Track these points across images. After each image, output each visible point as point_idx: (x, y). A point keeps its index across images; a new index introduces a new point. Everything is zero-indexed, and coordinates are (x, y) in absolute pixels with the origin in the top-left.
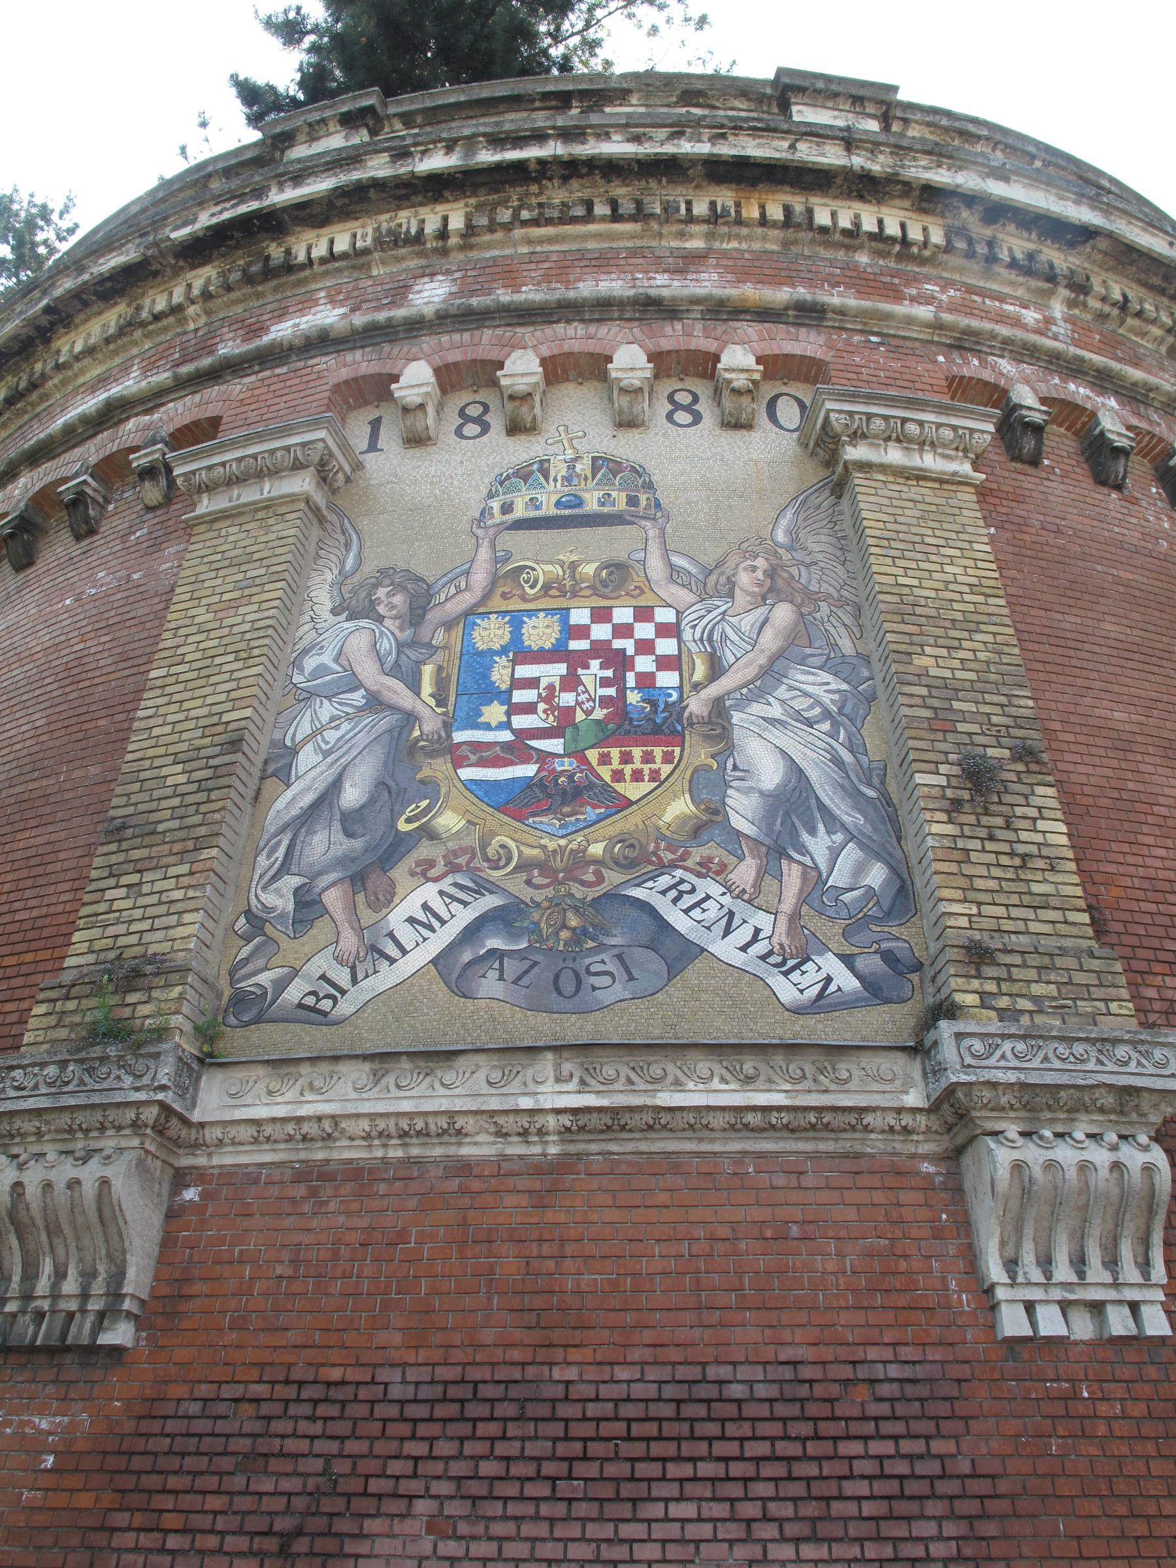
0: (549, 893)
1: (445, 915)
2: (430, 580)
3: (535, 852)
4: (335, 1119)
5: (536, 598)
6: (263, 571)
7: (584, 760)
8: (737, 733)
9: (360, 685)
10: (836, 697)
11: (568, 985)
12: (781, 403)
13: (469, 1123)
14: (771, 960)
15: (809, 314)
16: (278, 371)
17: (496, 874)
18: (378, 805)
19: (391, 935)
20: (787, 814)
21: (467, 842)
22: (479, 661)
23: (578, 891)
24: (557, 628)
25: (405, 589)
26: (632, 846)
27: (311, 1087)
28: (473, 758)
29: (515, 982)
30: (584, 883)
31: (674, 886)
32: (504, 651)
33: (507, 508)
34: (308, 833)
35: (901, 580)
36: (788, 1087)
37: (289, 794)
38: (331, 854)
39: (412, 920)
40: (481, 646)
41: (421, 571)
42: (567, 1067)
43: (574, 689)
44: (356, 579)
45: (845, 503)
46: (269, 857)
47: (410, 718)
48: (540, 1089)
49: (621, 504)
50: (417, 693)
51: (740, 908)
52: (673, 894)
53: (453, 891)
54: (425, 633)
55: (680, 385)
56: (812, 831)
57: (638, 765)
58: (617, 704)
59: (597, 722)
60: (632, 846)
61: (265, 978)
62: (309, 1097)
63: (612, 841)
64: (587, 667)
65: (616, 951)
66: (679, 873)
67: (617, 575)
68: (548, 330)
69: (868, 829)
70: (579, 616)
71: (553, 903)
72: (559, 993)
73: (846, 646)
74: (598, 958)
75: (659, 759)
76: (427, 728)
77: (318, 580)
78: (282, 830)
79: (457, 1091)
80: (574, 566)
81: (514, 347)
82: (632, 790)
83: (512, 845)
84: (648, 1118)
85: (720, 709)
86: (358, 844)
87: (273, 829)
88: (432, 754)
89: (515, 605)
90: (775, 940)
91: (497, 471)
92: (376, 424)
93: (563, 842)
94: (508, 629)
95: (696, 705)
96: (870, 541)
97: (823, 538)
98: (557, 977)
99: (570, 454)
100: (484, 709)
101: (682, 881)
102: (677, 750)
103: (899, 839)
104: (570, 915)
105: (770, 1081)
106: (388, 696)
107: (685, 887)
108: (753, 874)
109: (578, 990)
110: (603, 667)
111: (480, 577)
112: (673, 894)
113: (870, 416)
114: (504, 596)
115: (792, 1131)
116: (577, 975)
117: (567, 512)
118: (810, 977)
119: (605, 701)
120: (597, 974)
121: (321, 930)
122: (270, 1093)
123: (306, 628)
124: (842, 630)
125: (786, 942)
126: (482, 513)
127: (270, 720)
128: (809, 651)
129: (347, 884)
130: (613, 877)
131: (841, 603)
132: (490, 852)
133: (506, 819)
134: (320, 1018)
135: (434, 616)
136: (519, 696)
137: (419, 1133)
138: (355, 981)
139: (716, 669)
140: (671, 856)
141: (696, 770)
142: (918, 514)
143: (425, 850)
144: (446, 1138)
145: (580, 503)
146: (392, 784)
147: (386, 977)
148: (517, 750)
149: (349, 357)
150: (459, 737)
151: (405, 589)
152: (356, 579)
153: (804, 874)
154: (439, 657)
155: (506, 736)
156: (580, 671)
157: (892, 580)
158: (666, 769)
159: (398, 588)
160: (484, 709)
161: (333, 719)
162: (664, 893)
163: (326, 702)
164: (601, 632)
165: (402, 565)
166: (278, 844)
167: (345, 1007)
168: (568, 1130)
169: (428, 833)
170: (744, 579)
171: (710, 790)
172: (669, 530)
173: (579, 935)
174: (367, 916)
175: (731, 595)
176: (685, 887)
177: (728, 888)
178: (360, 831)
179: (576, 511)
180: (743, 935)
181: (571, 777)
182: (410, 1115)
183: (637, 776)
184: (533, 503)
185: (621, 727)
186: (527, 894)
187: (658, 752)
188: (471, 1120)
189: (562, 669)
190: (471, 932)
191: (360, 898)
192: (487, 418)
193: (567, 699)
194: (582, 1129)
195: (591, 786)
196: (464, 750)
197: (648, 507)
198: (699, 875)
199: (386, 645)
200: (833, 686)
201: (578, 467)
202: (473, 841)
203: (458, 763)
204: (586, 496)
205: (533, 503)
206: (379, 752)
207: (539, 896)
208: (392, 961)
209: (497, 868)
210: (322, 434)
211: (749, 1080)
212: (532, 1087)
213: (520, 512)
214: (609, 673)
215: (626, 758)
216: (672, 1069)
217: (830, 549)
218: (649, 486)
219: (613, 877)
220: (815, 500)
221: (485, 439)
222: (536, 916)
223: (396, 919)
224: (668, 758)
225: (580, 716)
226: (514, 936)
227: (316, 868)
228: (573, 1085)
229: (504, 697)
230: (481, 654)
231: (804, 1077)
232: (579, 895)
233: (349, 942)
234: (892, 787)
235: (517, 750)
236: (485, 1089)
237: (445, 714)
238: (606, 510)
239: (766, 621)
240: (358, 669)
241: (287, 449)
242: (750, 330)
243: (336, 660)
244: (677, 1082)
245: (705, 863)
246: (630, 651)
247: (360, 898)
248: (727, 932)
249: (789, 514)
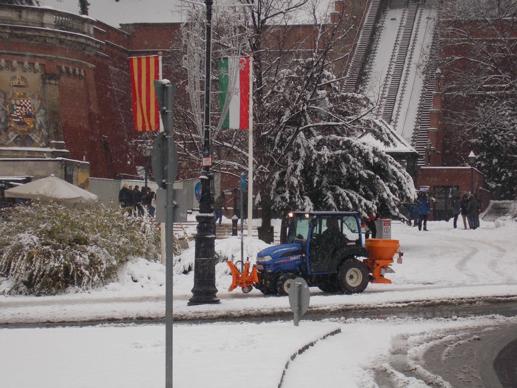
22: (12, 106)
47: (7, 112)
70: (22, 101)
80: (20, 93)
82: (28, 123)
95: (33, 114)
111: (11, 94)
118: (42, 144)
135: (7, 98)
139: (34, 109)
143: (11, 128)
148: (17, 118)
150: (12, 115)
169: (11, 126)
170: (36, 97)
171: (34, 123)
190: (17, 138)
193: (21, 112)
199: (3, 101)
213: (14, 84)
218: (27, 82)
223: (9, 135)
235: (17, 118)
242: (38, 59)
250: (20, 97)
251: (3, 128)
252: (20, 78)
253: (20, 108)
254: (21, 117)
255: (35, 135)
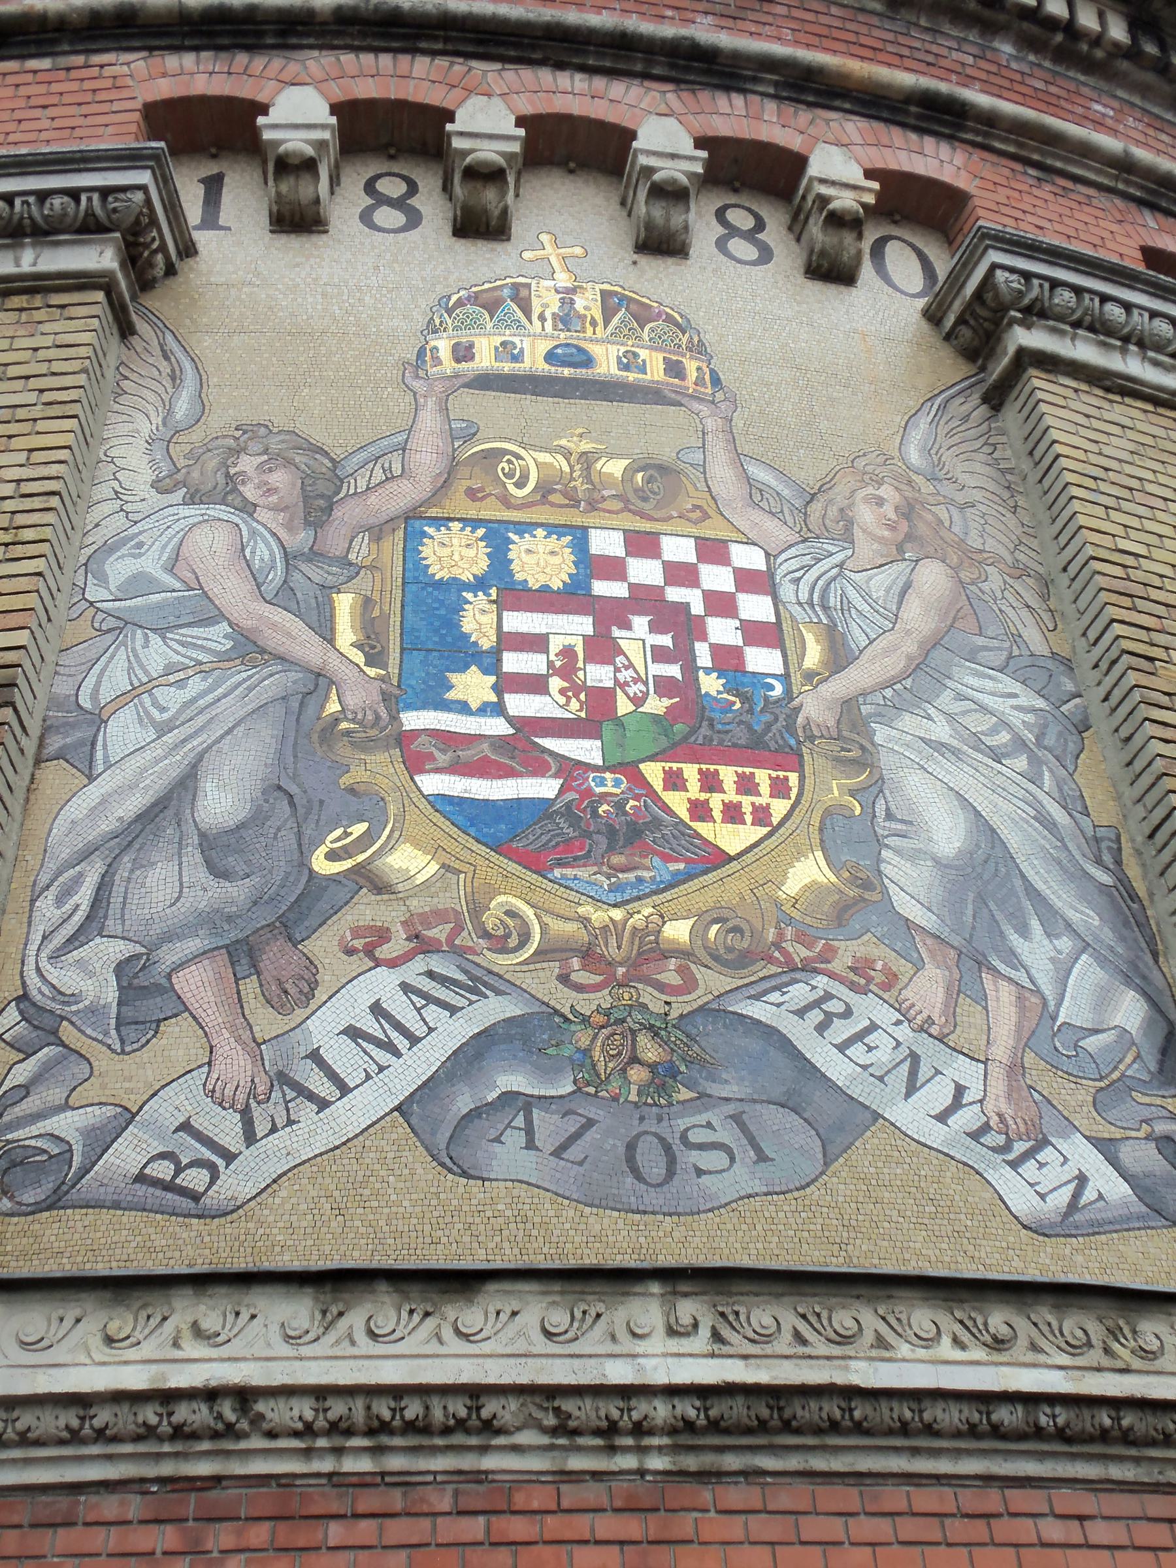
0: (603, 998)
1: (419, 1029)
2: (338, 453)
3: (571, 927)
4: (244, 1396)
5: (525, 505)
6: (32, 397)
7: (638, 780)
8: (886, 761)
9: (219, 616)
10: (1030, 718)
11: (652, 1162)
12: (892, 248)
13: (506, 1410)
14: (990, 1139)
15: (939, 116)
16: (33, 64)
17: (502, 962)
18: (274, 822)
19: (315, 1056)
20: (981, 899)
21: (444, 901)
23: (653, 1000)
24: (568, 556)
25: (289, 462)
26: (736, 929)
27: (197, 1331)
28: (443, 759)
29: (558, 1153)
30: (661, 987)
31: (817, 1004)
32: (480, 584)
33: (463, 353)
34: (136, 865)
35: (1123, 544)
36: (1064, 1359)
37: (94, 792)
38: (185, 905)
39: (353, 1033)
40: (439, 573)
41: (318, 436)
42: (687, 1309)
43: (610, 661)
44: (196, 435)
45: (1011, 416)
46: (59, 901)
47: (319, 681)
48: (640, 1347)
49: (656, 371)
50: (329, 638)
51: (927, 1047)
52: (816, 1016)
53: (427, 985)
54: (334, 540)
55: (732, 199)
56: (1024, 931)
57: (731, 796)
58: (683, 690)
59: (655, 718)
60: (736, 929)
61: (67, 1125)
62: (192, 1349)
63: (704, 919)
64: (627, 626)
65: (730, 1109)
66: (821, 981)
67: (659, 487)
68: (527, 74)
69: (1108, 935)
70: (606, 542)
71: (611, 1019)
72: (639, 1177)
73: (1034, 638)
74: (702, 1119)
75: (765, 788)
76: (352, 701)
77: (125, 428)
78: (86, 855)
79: (486, 1348)
80: (587, 460)
81: (470, 91)
83: (529, 913)
84: (832, 1408)
85: (852, 718)
86: (237, 892)
87: (65, 854)
88: (366, 745)
89: (491, 511)
90: (989, 1106)
91: (440, 290)
92: (213, 186)
93: (617, 914)
94: (483, 549)
95: (815, 707)
96: (1069, 477)
97: (978, 468)
98: (631, 1147)
99: (563, 279)
100: (454, 678)
101: (828, 996)
102: (793, 778)
103: (1155, 955)
104: (643, 1040)
105: (1034, 1347)
106: (273, 640)
107: (834, 1006)
108: (941, 995)
109: (671, 1173)
110: (654, 628)
111: (427, 458)
112: (816, 1016)
113: (1055, 284)
114: (471, 494)
115: (1069, 1440)
116: (667, 1148)
117: (567, 372)
119: (664, 686)
120: (701, 1147)
121: (177, 1042)
122: (110, 1341)
123: (107, 508)
124: (1025, 613)
125: (1004, 1107)
126: (421, 353)
127: (50, 658)
128: (980, 641)
129: (222, 958)
130: (712, 981)
131: (1020, 572)
132: (490, 920)
133: (513, 867)
134: (186, 1204)
135: (347, 514)
136: (513, 662)
137: (410, 1427)
138: (250, 1138)
140: (804, 953)
141: (828, 813)
142: (1132, 446)
143: (366, 910)
144: (458, 1439)
145: (588, 361)
146: (293, 789)
147: (312, 1133)
149: (172, 61)
151: (289, 462)
152: (196, 435)
153: (1020, 999)
154: (364, 581)
155: (498, 727)
156: (616, 632)
157: (1107, 541)
158: (779, 808)
159: (275, 459)
160: (454, 678)
161: (170, 670)
162: (801, 1013)
163: (155, 639)
164: (644, 571)
165: (279, 421)
166: (78, 880)
167: (235, 1184)
168: (689, 1426)
169: (369, 880)
172: (738, 423)
173: (663, 1078)
174: (266, 1022)
175: (848, 538)
176: (834, 1006)
177: (905, 1014)
178: (241, 868)
179: (581, 373)
180: (938, 1094)
181: (620, 806)
182: (397, 1392)
183: (733, 814)
184: (507, 351)
185: (693, 730)
186: (564, 999)
187: (763, 777)
188: (513, 1404)
189: (584, 625)
191: (250, 987)
192: (414, 201)
193: (599, 675)
194: (715, 1426)
195: (656, 823)
196: (422, 744)
197: (699, 382)
198: (853, 987)
199: (263, 552)
200: (1022, 701)
201: (580, 304)
202: (455, 898)
203: (416, 764)
204: (596, 350)
205: (507, 351)
206: (266, 733)
207: (587, 1004)
208: (324, 1105)
209: (504, 950)
210: (144, 177)
211: (998, 1344)
212: (627, 1344)
214: (666, 640)
215: (711, 783)
216: (869, 1319)
217: (991, 486)
218: (699, 349)
219: (712, 981)
220: (958, 407)
221: (414, 235)
222: (584, 1042)
223: (323, 1028)
224: (779, 789)
225: (624, 706)
226: (549, 1072)
227: (156, 929)
228: (701, 1341)
229: (490, 662)
230: (440, 584)
231: (1089, 1344)
232: (657, 1007)
233: (235, 1066)
234: (1133, 870)
236: (541, 1345)
237: (382, 679)
238: (632, 377)
239: (907, 586)
240: (214, 589)
241: (74, 194)
243: (171, 569)
244: (881, 1342)
245: (862, 967)
246: (697, 608)
247: (250, 987)
248: (912, 1088)
249: (923, 422)
250: (569, 502)
251: (211, 920)
252: (587, 303)
253: (571, 629)
254: (587, 750)
255: (872, 1008)
